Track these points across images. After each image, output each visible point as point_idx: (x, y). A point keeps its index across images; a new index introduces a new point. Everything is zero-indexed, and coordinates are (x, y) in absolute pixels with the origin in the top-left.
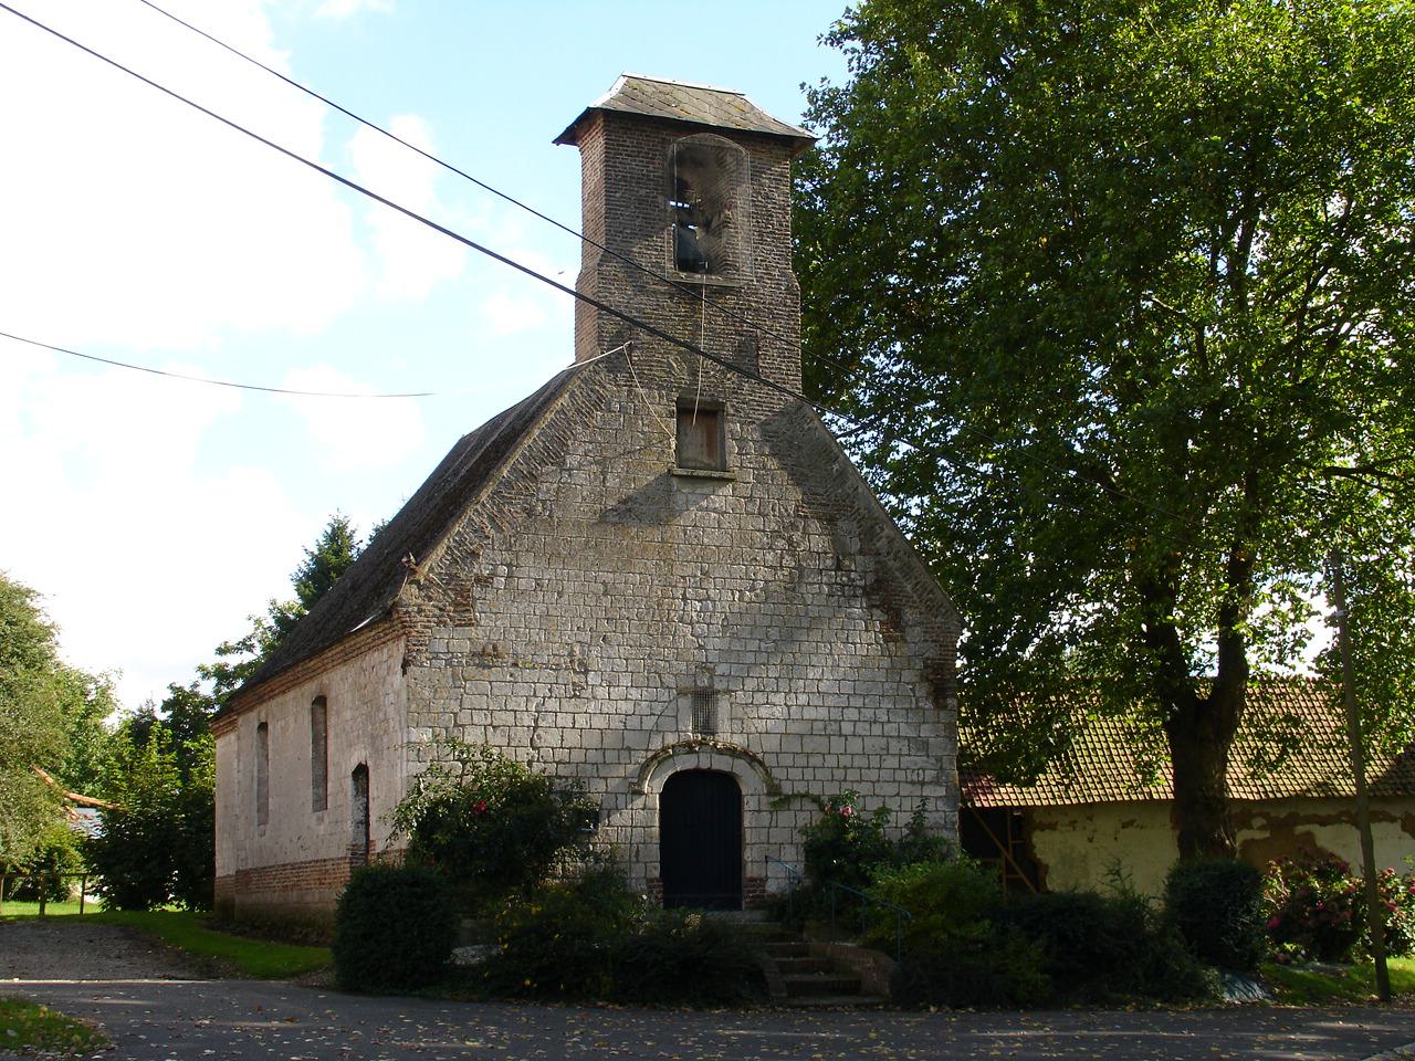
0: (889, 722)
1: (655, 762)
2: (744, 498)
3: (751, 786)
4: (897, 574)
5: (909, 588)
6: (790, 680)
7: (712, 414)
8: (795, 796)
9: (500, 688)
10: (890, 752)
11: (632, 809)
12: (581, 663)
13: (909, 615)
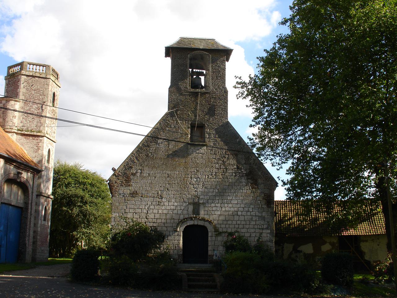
0: (253, 211)
1: (181, 223)
2: (210, 150)
3: (210, 229)
4: (256, 169)
5: (260, 173)
6: (222, 200)
7: (201, 127)
8: (223, 232)
9: (137, 203)
10: (253, 220)
11: (174, 235)
12: (160, 196)
13: (260, 181)
